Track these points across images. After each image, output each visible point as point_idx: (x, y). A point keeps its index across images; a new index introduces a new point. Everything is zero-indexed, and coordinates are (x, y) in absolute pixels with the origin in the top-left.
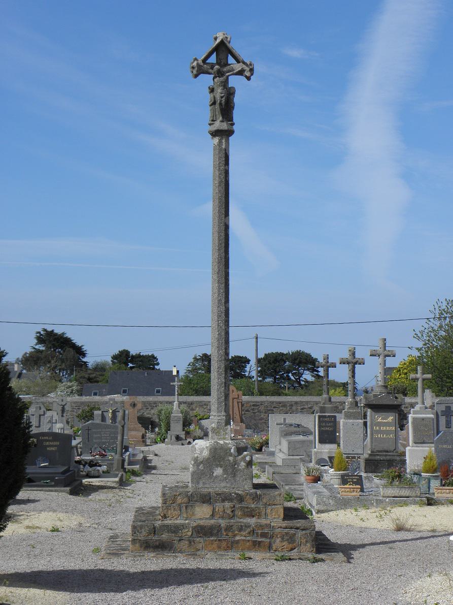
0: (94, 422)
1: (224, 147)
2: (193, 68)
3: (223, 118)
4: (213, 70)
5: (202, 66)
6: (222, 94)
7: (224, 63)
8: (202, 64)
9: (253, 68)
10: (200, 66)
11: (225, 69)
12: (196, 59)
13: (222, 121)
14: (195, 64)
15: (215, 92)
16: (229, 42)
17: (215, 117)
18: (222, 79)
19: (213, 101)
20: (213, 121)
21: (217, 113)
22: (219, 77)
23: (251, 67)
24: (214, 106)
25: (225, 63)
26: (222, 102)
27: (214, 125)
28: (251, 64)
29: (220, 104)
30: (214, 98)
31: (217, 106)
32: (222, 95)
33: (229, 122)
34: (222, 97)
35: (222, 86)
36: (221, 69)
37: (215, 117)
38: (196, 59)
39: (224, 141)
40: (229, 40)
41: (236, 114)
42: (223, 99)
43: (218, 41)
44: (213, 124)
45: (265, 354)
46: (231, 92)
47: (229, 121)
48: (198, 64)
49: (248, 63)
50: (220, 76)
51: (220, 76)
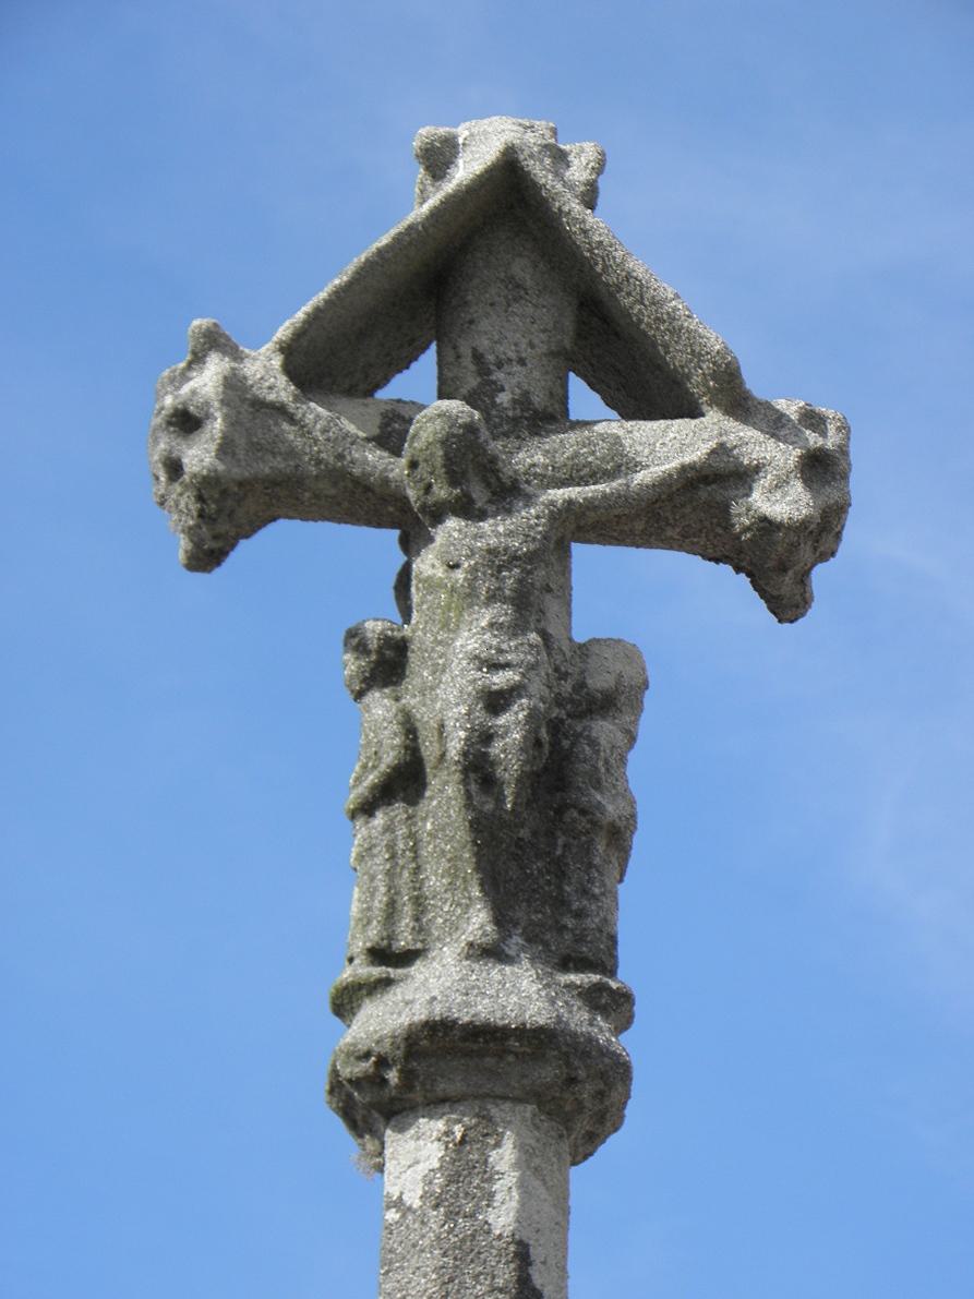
0: (270, 345)
1: (502, 1217)
2: (186, 422)
3: (501, 919)
4: (397, 452)
5: (280, 410)
6: (495, 666)
7: (523, 401)
8: (281, 389)
9: (843, 450)
10: (259, 405)
11: (530, 456)
12: (213, 341)
13: (489, 953)
14: (208, 380)
15: (419, 671)
16: (590, 198)
17: (405, 923)
18: (494, 530)
19: (389, 758)
20: (379, 955)
21: (434, 881)
22: (467, 510)
23: (813, 439)
24: (399, 809)
25: (539, 399)
26: (496, 749)
27: (396, 994)
28: (813, 420)
29: (478, 768)
30: (410, 729)
31: (444, 796)
32: (500, 679)
33: (574, 978)
34: (496, 702)
35: (492, 598)
36: (484, 434)
37: (405, 923)
38: (213, 341)
39: (504, 1156)
40: (578, 172)
41: (647, 910)
42: (512, 725)
43: (465, 170)
44: (387, 983)
45: (737, 573)
46: (599, 682)
47: (583, 965)
48: (234, 385)
49: (790, 408)
50: (480, 495)
51: (480, 495)
